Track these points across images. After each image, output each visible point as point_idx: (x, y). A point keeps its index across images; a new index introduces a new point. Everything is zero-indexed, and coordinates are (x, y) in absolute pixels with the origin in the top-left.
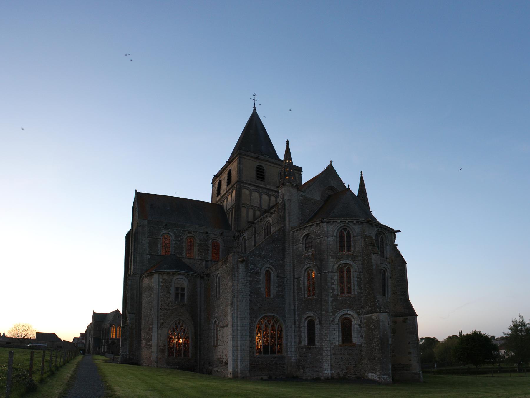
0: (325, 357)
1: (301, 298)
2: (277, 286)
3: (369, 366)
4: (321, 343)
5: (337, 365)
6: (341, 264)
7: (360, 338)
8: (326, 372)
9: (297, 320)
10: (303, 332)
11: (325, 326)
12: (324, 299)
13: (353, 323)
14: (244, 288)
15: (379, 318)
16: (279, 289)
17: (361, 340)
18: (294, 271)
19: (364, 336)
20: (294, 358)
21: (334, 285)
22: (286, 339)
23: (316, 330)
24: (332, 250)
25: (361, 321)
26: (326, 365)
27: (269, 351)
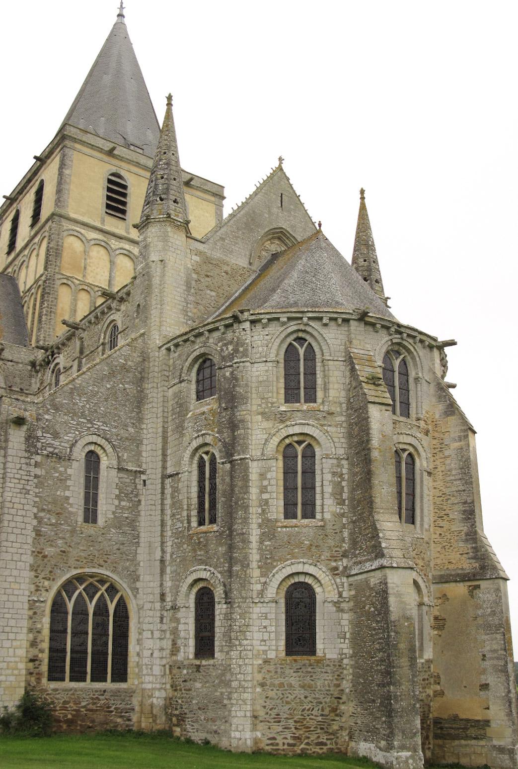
0: (236, 692)
1: (180, 529)
2: (117, 496)
3: (359, 722)
4: (227, 653)
6: (287, 437)
8: (238, 735)
10: (182, 621)
11: (238, 606)
13: (319, 598)
15: (386, 584)
16: (123, 503)
18: (164, 455)
19: (348, 635)
20: (157, 694)
22: (139, 641)
23: (217, 618)
25: (340, 595)
27: (86, 673)
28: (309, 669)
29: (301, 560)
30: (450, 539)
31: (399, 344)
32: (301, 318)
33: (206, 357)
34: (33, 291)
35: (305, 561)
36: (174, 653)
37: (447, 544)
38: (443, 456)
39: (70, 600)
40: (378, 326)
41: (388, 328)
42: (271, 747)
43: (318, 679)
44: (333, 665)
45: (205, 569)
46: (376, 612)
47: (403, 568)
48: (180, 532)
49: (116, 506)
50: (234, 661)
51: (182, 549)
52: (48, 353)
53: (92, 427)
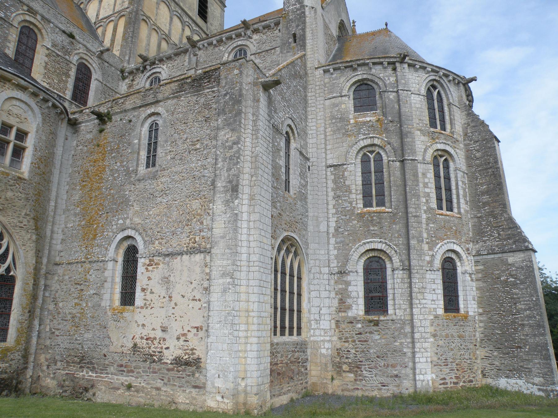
0: (419, 342)
1: (347, 208)
5: (441, 360)
8: (421, 377)
11: (417, 273)
12: (414, 214)
13: (459, 270)
20: (327, 345)
26: (421, 360)
28: (462, 324)
42: (442, 386)
48: (348, 210)
51: (351, 224)
52: (146, 63)
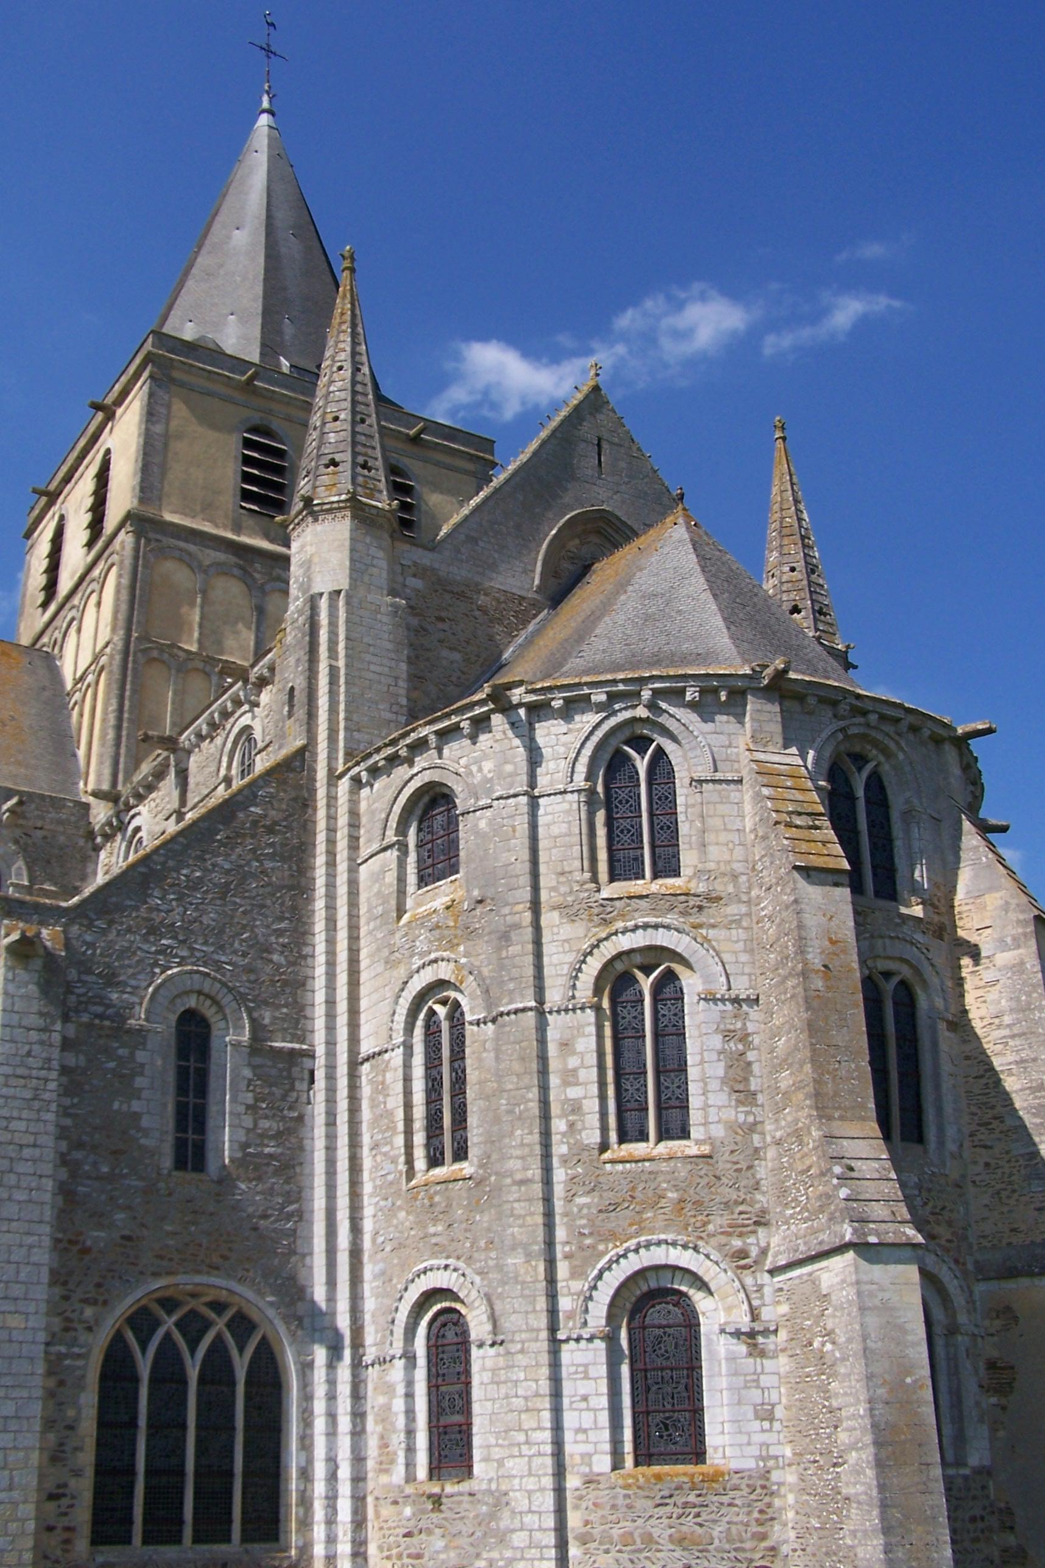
0: (522, 1558)
1: (390, 1177)
2: (248, 1107)
4: (500, 1463)
6: (619, 956)
7: (756, 1425)
9: (367, 1317)
11: (522, 1351)
12: (518, 1176)
13: (707, 1326)
14: (25, 1114)
16: (265, 1124)
17: (765, 1437)
19: (779, 1412)
21: (577, 1084)
24: (562, 874)
25: (755, 1316)
27: (181, 1522)
28: (692, 1498)
29: (663, 1237)
30: (1011, 1175)
31: (863, 737)
32: (638, 694)
33: (437, 789)
34: (90, 678)
35: (670, 1237)
36: (384, 1466)
37: (1003, 1186)
38: (982, 983)
39: (144, 1350)
40: (812, 701)
41: (834, 704)
43: (715, 1521)
44: (748, 1486)
45: (446, 1267)
46: (838, 1355)
47: (894, 1245)
48: (391, 1183)
49: (248, 1131)
50: (516, 1481)
53: (189, 957)
